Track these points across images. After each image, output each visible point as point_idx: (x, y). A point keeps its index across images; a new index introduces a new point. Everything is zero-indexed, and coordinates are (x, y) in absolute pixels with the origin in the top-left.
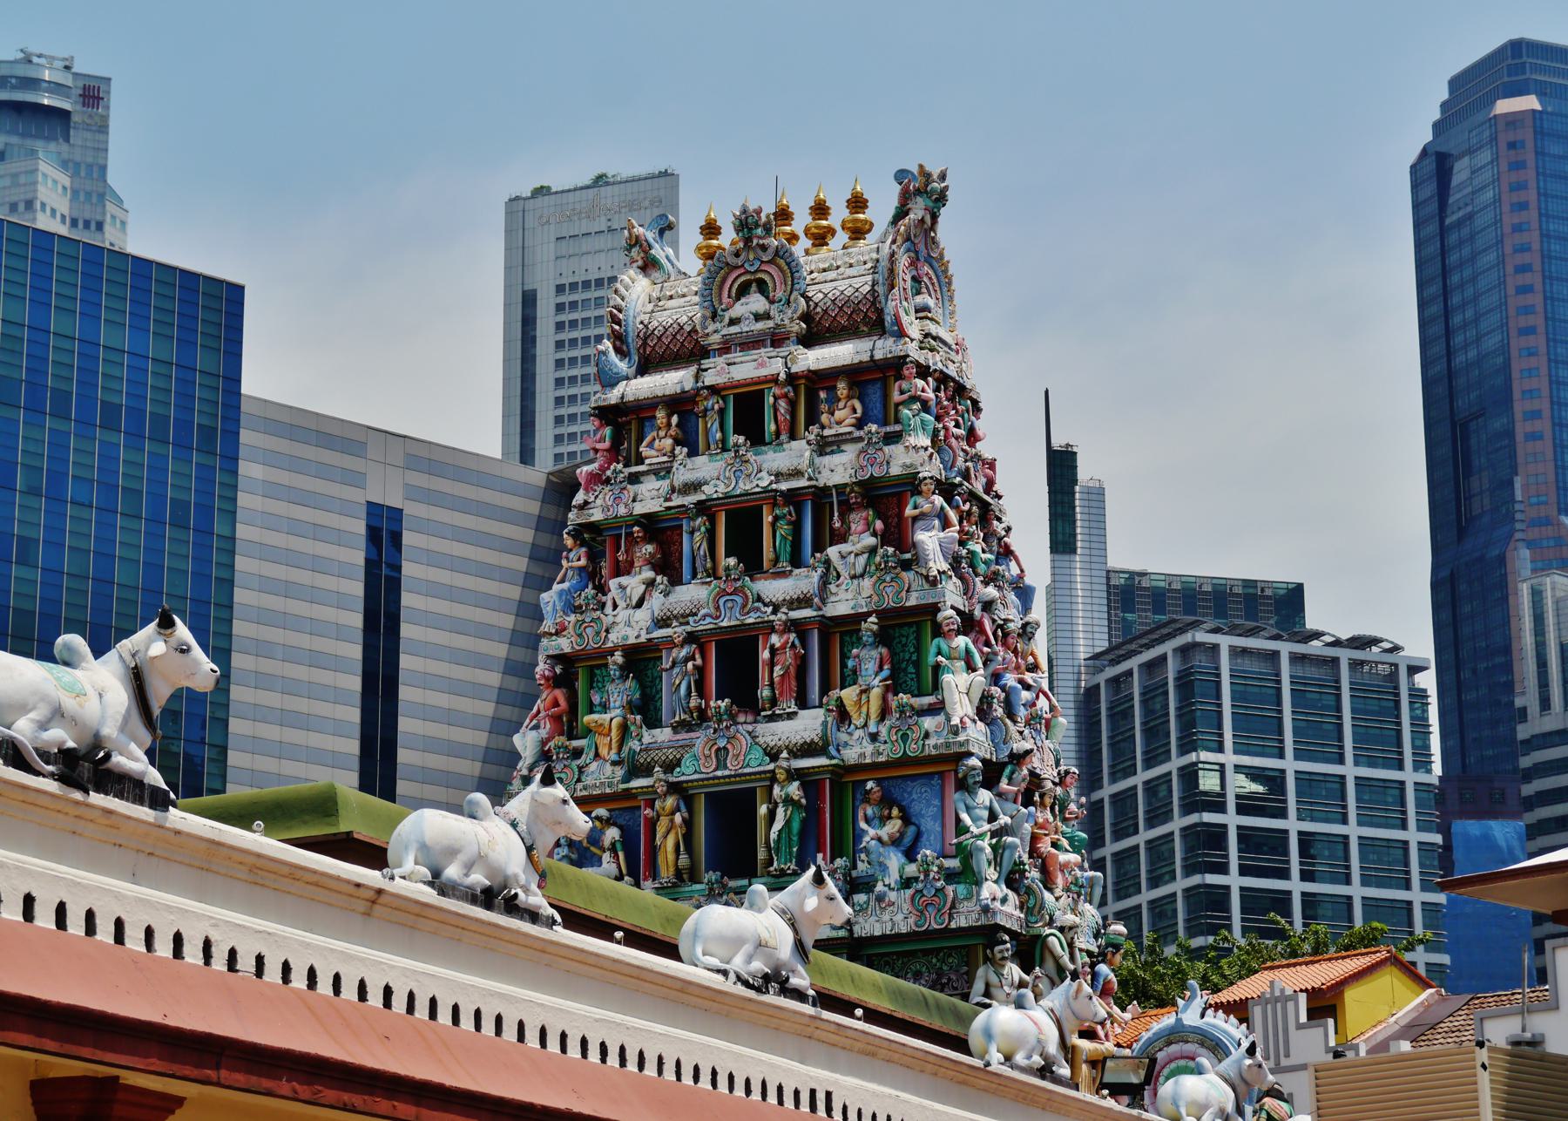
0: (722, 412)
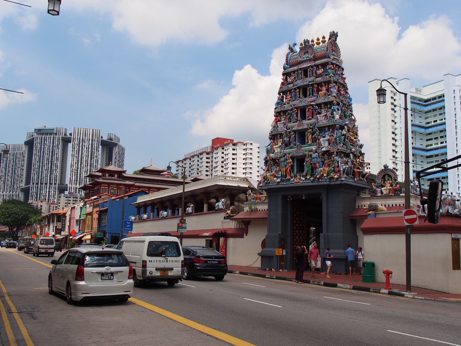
0: (301, 73)
